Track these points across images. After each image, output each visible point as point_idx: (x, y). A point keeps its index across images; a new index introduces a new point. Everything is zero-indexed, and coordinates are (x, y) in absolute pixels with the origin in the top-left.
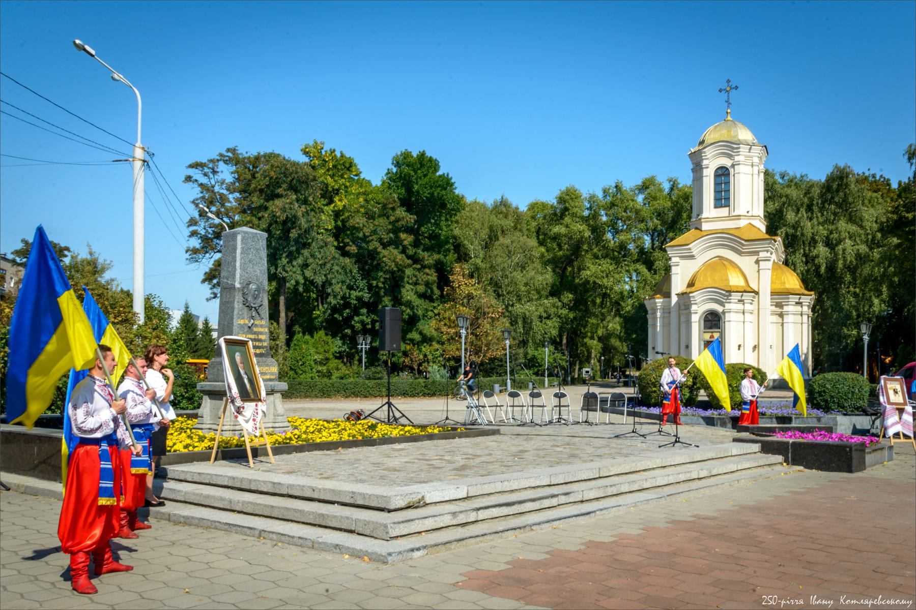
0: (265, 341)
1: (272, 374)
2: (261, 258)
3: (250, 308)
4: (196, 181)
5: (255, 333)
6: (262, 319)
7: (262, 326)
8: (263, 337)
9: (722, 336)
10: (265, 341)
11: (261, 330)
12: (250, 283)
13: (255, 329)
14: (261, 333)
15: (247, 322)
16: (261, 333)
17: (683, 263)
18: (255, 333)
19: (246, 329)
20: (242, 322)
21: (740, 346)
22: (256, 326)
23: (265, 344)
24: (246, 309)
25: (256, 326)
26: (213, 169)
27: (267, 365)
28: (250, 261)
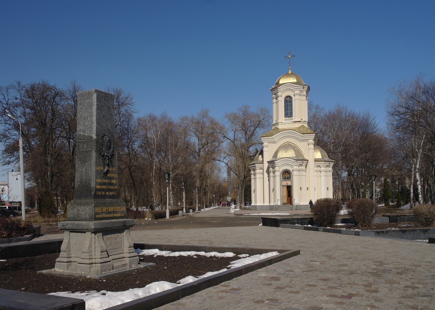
0: (115, 185)
1: (122, 212)
8: (114, 181)
9: (292, 183)
10: (115, 185)
17: (270, 145)
21: (308, 188)
23: (116, 187)
27: (119, 205)
28: (104, 117)
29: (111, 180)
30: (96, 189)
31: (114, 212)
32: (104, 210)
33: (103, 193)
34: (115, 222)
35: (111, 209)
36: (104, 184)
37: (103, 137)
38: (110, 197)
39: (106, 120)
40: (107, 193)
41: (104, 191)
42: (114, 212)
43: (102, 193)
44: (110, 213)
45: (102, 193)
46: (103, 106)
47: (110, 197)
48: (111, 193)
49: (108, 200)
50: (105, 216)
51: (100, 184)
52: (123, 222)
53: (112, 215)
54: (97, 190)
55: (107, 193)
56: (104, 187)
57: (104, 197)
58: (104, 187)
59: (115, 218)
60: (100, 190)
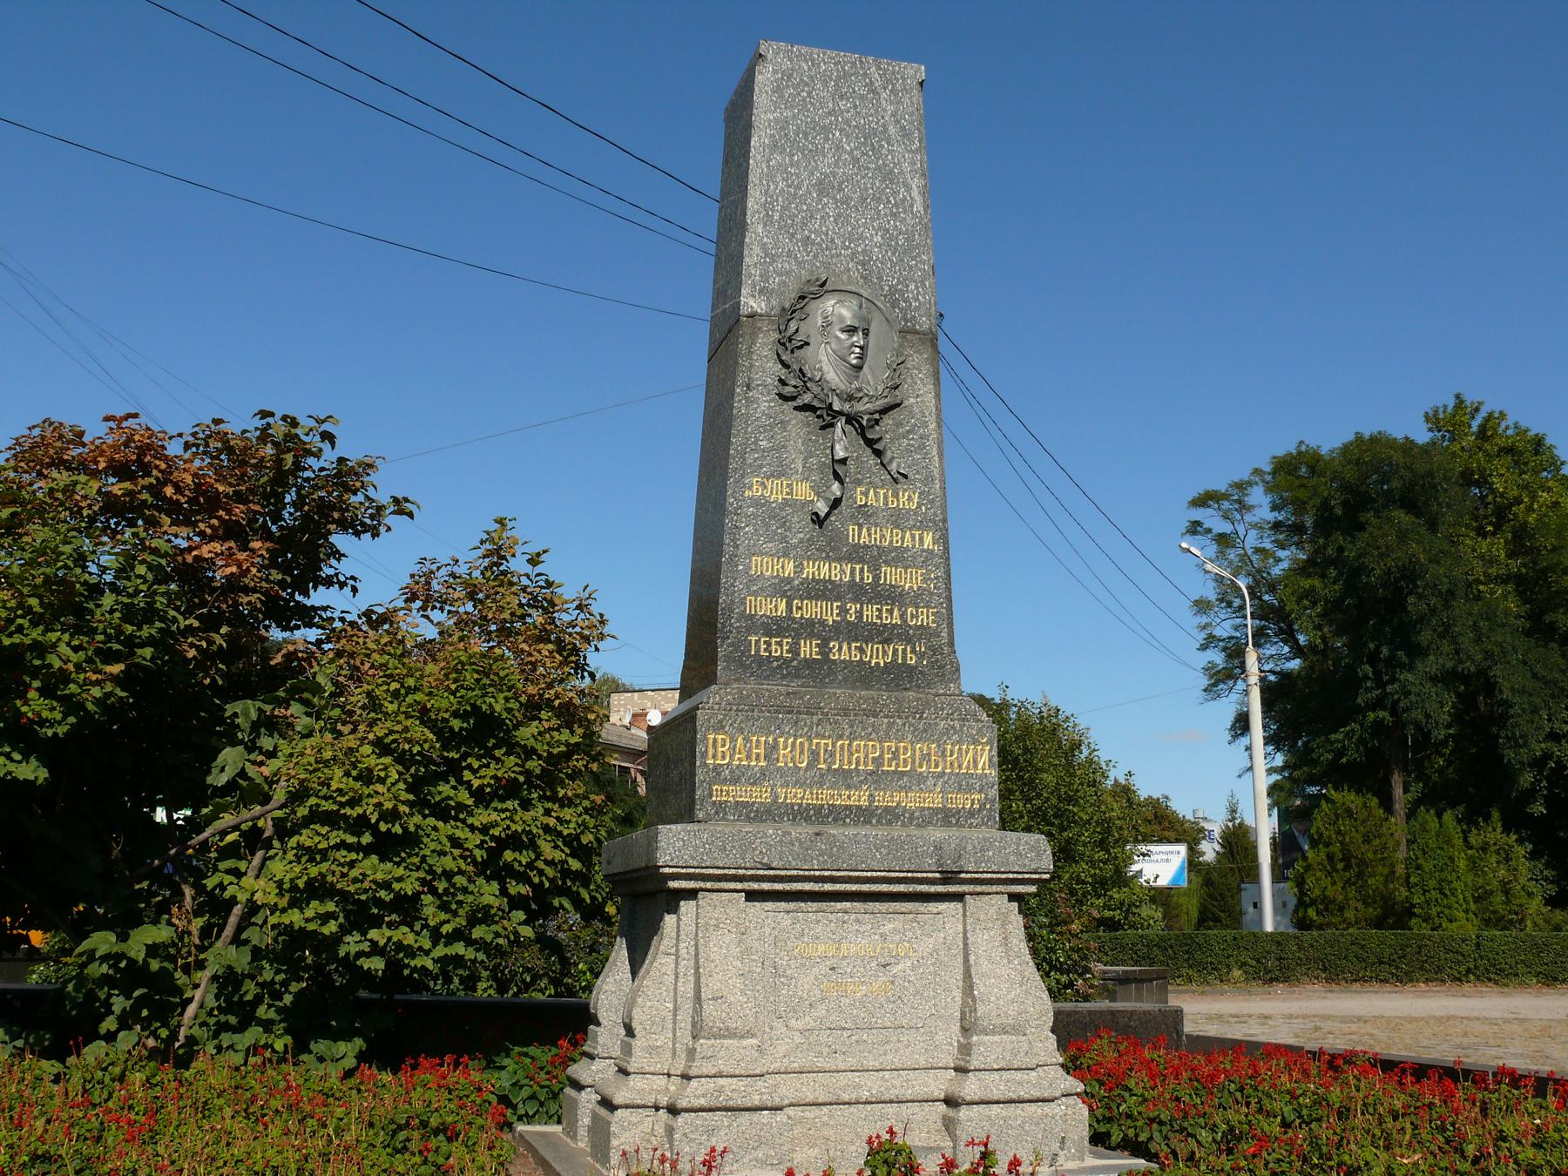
1: (963, 783)
2: (888, 176)
3: (824, 416)
4: (1209, 531)
5: (856, 554)
6: (898, 479)
7: (897, 519)
11: (891, 537)
13: (856, 535)
15: (803, 491)
16: (899, 557)
18: (856, 554)
19: (801, 530)
20: (775, 491)
22: (865, 515)
24: (798, 426)
25: (865, 515)
26: (1239, 501)
27: (924, 734)
28: (823, 188)
29: (875, 569)
31: (877, 777)
32: (791, 750)
33: (809, 649)
35: (862, 752)
36: (821, 590)
37: (817, 297)
39: (846, 201)
40: (843, 652)
41: (811, 636)
42: (877, 777)
43: (794, 650)
44: (845, 778)
45: (794, 650)
46: (826, 130)
47: (863, 675)
48: (877, 655)
50: (795, 795)
51: (782, 588)
52: (938, 848)
53: (859, 797)
54: (754, 624)
55: (843, 652)
56: (810, 610)
58: (810, 610)
60: (775, 628)
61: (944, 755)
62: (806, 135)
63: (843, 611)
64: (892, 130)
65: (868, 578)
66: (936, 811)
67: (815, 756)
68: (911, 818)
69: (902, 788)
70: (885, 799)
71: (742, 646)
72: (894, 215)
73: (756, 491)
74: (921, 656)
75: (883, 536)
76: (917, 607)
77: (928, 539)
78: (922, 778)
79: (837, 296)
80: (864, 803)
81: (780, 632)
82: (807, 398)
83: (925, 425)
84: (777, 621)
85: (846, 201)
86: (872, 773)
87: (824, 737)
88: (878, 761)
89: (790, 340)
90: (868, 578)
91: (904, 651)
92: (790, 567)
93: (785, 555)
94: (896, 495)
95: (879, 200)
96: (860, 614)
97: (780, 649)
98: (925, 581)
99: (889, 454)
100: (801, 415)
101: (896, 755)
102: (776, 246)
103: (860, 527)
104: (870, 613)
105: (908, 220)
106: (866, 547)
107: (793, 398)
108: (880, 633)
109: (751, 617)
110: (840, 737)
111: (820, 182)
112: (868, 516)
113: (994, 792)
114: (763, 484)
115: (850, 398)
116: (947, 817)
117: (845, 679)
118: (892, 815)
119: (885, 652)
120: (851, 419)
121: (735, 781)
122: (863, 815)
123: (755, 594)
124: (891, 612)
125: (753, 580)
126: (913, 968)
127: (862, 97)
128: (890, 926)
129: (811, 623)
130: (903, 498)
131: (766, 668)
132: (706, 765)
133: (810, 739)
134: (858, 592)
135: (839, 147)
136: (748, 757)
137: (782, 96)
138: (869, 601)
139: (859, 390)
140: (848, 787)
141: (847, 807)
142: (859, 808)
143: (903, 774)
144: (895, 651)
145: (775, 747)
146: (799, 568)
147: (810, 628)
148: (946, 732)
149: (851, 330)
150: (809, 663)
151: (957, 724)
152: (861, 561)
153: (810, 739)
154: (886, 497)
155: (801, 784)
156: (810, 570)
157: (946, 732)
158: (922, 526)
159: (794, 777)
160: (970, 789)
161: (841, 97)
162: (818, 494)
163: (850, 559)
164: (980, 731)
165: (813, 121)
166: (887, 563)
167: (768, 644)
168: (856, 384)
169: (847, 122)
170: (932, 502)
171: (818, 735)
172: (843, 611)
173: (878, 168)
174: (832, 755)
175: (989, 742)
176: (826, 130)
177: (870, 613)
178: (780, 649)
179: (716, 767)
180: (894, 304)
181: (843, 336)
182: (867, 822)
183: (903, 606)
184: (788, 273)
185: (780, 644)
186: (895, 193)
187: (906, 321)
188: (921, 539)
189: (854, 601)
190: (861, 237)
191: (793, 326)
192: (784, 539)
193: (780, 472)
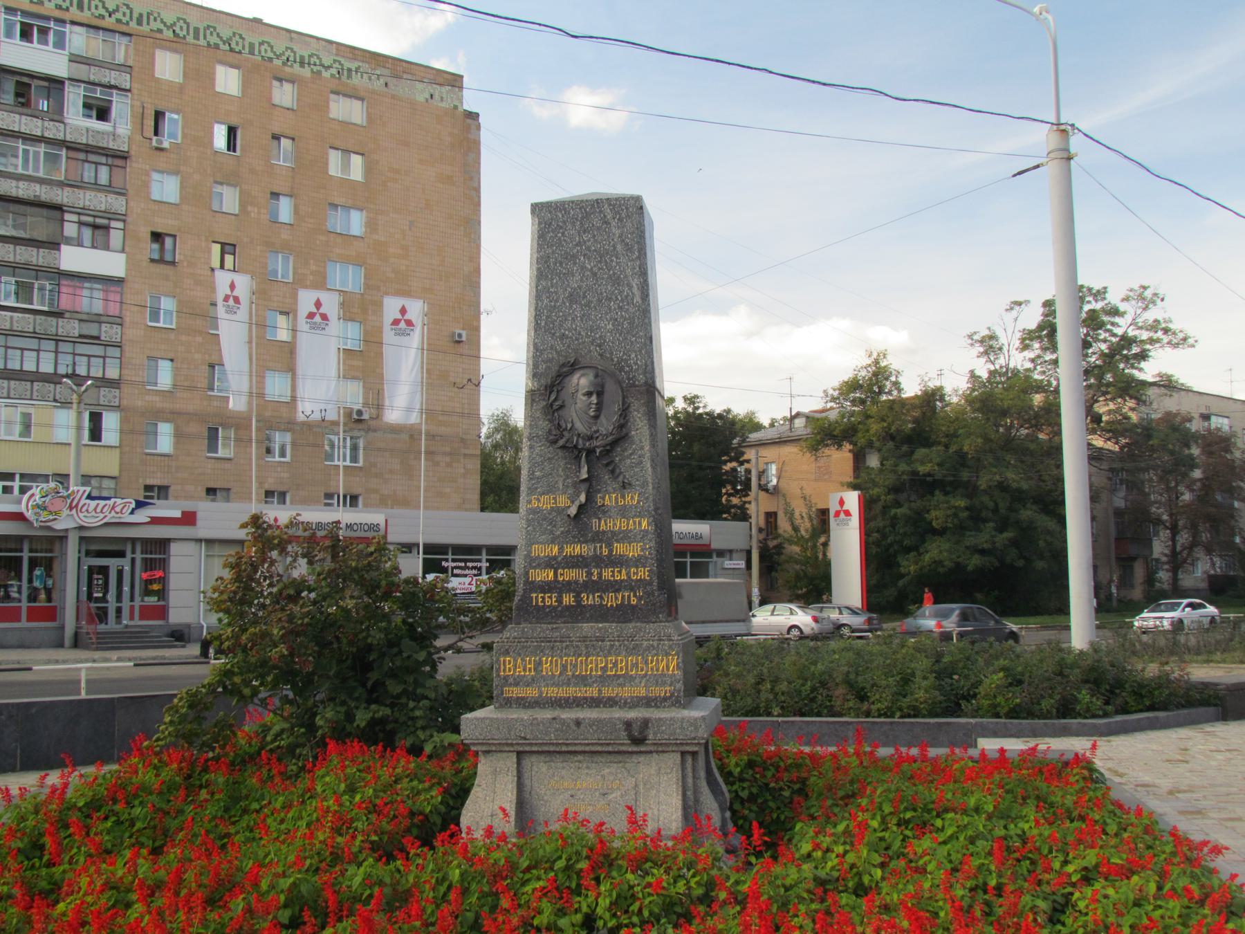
0: (639, 562)
1: (659, 680)
2: (616, 281)
3: (573, 452)
5: (598, 537)
6: (624, 486)
8: (632, 550)
11: (619, 524)
12: (573, 367)
14: (625, 537)
15: (563, 501)
16: (625, 537)
20: (545, 503)
22: (603, 511)
23: (643, 573)
25: (603, 511)
27: (635, 650)
28: (572, 298)
29: (609, 545)
30: (527, 582)
31: (604, 680)
32: (549, 665)
33: (568, 599)
34: (578, 723)
35: (593, 664)
38: (601, 614)
39: (588, 304)
40: (588, 599)
41: (569, 591)
42: (604, 680)
43: (560, 600)
44: (583, 680)
45: (560, 600)
46: (574, 257)
48: (611, 600)
49: (587, 628)
50: (552, 692)
51: (551, 563)
52: (628, 724)
53: (592, 692)
54: (532, 586)
55: (588, 599)
56: (569, 575)
57: (577, 613)
58: (569, 575)
59: (611, 702)
60: (546, 587)
61: (646, 663)
62: (561, 264)
63: (590, 574)
64: (619, 247)
65: (605, 552)
66: (641, 698)
67: (564, 667)
68: (626, 703)
69: (620, 685)
70: (608, 692)
71: (526, 599)
72: (620, 308)
73: (535, 504)
74: (640, 599)
75: (615, 524)
76: (637, 567)
77: (644, 524)
78: (632, 678)
79: (581, 372)
80: (595, 694)
81: (550, 590)
82: (561, 442)
83: (642, 448)
84: (548, 583)
85: (588, 304)
86: (600, 676)
87: (568, 656)
88: (604, 669)
89: (551, 405)
90: (605, 552)
91: (629, 597)
92: (556, 549)
93: (553, 542)
94: (623, 497)
95: (610, 300)
96: (600, 574)
97: (550, 600)
98: (642, 550)
99: (618, 471)
100: (560, 453)
101: (615, 664)
102: (543, 344)
103: (600, 519)
104: (607, 574)
105: (631, 310)
106: (604, 532)
107: (555, 442)
108: (613, 586)
109: (533, 582)
110: (580, 655)
111: (571, 295)
112: (604, 513)
113: (680, 686)
114: (539, 500)
115: (591, 438)
116: (649, 702)
117: (591, 616)
118: (611, 702)
119: (616, 598)
120: (590, 452)
121: (517, 684)
122: (595, 703)
123: (535, 568)
124: (620, 572)
125: (532, 560)
126: (622, 796)
127: (599, 228)
128: (607, 771)
129: (569, 583)
130: (628, 498)
131: (543, 614)
132: (498, 676)
133: (561, 658)
134: (599, 561)
135: (583, 268)
136: (525, 670)
137: (545, 240)
138: (606, 566)
139: (597, 431)
140: (585, 686)
141: (585, 698)
142: (592, 698)
143: (619, 676)
144: (623, 597)
145: (540, 663)
146: (561, 549)
147: (569, 586)
148: (648, 649)
149: (589, 394)
150: (569, 607)
151: (655, 644)
152: (601, 541)
153: (561, 658)
154: (616, 499)
155: (558, 685)
156: (568, 550)
157: (648, 649)
158: (641, 516)
159: (552, 681)
160: (664, 683)
161: (585, 232)
162: (573, 502)
163: (593, 541)
164: (670, 647)
165: (566, 253)
166: (618, 541)
167: (543, 598)
168: (594, 428)
169: (588, 248)
170: (647, 498)
171: (566, 655)
172: (590, 574)
173: (610, 277)
174: (575, 666)
175: (677, 654)
176: (574, 257)
177: (607, 574)
178: (550, 600)
179: (506, 678)
180: (621, 369)
181: (584, 398)
182: (598, 706)
183: (628, 567)
184: (550, 361)
185: (550, 597)
186: (621, 292)
187: (629, 379)
188: (640, 523)
189: (596, 567)
190: (599, 327)
191: (553, 397)
192: (551, 532)
193: (551, 490)
